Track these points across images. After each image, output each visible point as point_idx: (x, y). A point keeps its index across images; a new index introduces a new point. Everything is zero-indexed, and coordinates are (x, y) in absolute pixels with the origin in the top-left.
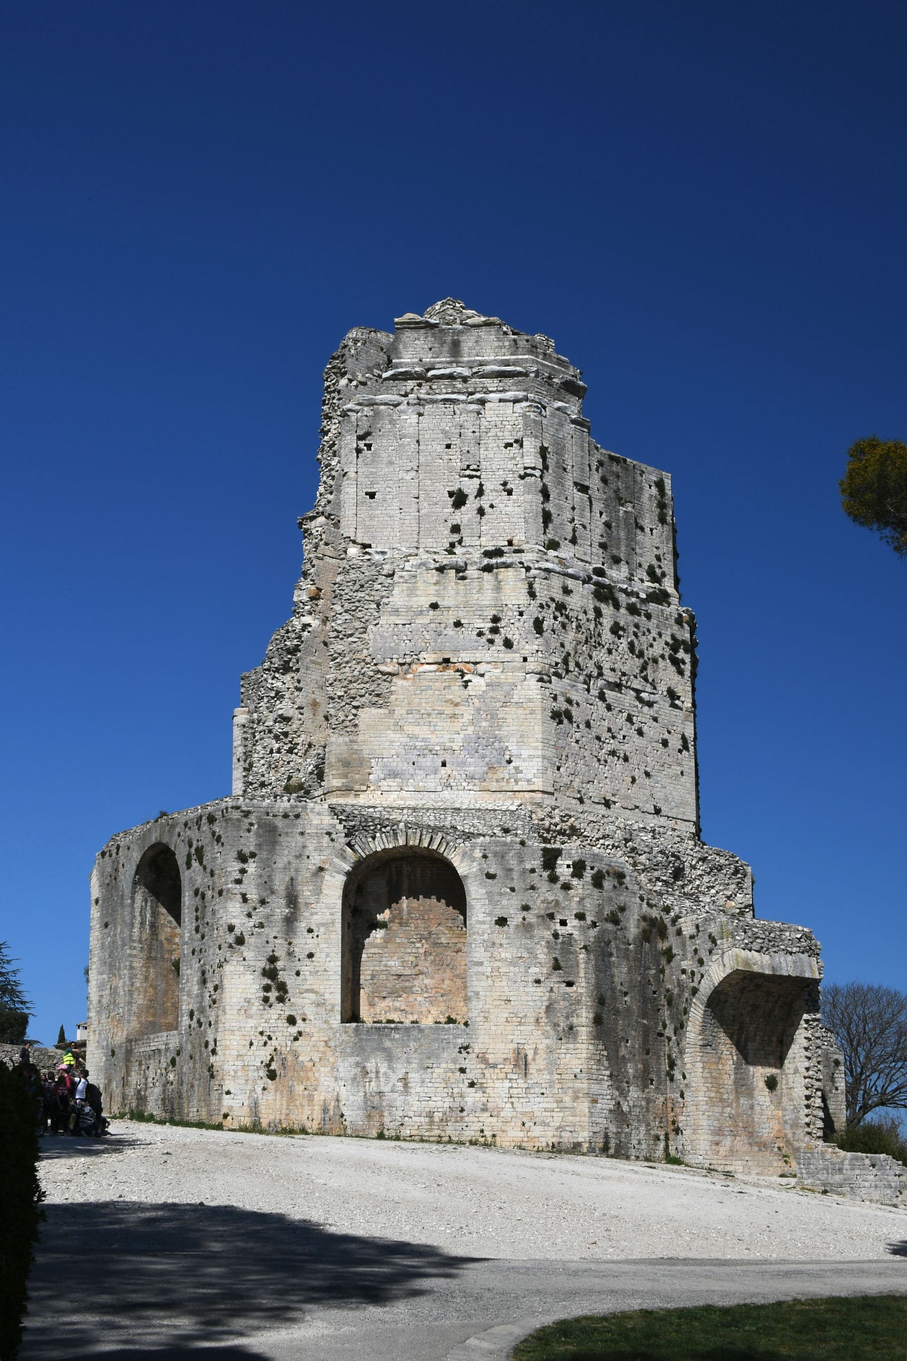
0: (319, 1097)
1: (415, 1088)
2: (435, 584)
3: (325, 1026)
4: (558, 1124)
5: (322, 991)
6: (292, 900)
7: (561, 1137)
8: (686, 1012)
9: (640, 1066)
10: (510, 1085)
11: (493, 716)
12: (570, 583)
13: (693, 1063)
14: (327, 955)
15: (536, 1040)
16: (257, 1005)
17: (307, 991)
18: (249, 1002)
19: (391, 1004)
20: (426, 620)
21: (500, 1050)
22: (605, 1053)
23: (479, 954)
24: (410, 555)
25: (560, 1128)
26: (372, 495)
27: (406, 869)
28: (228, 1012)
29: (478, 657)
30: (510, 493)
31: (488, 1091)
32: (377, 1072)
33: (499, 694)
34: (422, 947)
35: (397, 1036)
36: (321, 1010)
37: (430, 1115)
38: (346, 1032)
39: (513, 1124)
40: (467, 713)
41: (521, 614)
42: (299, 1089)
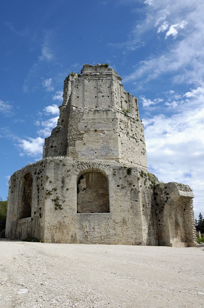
0: (71, 233)
1: (96, 230)
2: (94, 114)
3: (72, 214)
4: (135, 238)
5: (71, 205)
6: (63, 182)
7: (136, 241)
8: (163, 207)
9: (152, 221)
10: (122, 228)
11: (107, 142)
12: (122, 114)
13: (167, 220)
14: (73, 196)
15: (129, 216)
16: (53, 209)
17: (67, 205)
18: (51, 208)
19: (87, 209)
20: (91, 122)
21: (119, 219)
22: (145, 218)
23: (112, 193)
24: (87, 109)
25: (136, 239)
26: (78, 97)
27: (90, 175)
28: (46, 211)
29: (104, 129)
30: (109, 97)
31: (116, 230)
32: (86, 226)
33: (108, 137)
34: (95, 194)
35: (91, 216)
36: (71, 210)
37: (101, 237)
38: (77, 216)
39: (123, 238)
40: (101, 141)
41: (113, 120)
42: (65, 231)
